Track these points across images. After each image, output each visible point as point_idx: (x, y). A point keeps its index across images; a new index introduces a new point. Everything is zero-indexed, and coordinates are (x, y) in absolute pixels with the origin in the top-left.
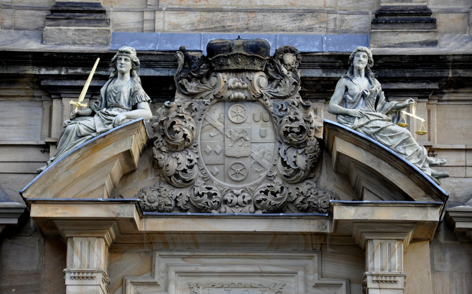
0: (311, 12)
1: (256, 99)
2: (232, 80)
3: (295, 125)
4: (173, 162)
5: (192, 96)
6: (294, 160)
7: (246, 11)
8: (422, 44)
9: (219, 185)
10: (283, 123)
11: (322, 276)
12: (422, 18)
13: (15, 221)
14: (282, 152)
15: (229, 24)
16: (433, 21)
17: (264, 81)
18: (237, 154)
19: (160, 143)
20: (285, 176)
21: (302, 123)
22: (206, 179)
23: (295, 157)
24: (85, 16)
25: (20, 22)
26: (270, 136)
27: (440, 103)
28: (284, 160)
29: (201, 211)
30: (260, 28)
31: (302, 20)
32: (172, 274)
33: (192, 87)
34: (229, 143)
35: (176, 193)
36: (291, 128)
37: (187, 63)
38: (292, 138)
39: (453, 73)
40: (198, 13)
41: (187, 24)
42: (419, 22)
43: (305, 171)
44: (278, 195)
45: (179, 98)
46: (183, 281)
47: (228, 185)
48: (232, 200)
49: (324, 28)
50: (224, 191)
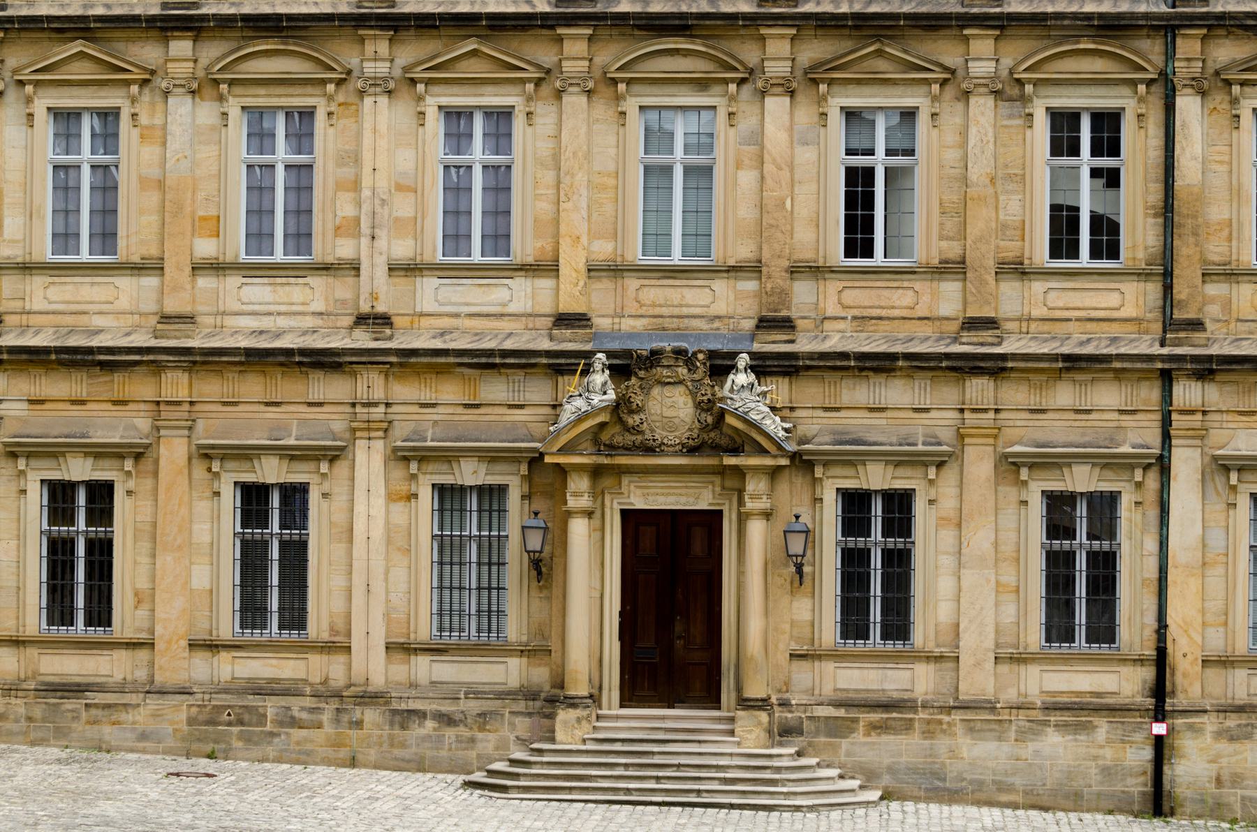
0: (719, 317)
1: (681, 382)
2: (665, 372)
3: (705, 398)
4: (632, 420)
11: (723, 488)
12: (787, 324)
16: (793, 328)
17: (685, 371)
19: (623, 408)
21: (709, 396)
24: (577, 323)
25: (538, 325)
26: (690, 404)
29: (649, 450)
30: (686, 329)
32: (632, 487)
33: (642, 374)
35: (634, 438)
42: (784, 327)
45: (633, 380)
46: (639, 492)
47: (665, 434)
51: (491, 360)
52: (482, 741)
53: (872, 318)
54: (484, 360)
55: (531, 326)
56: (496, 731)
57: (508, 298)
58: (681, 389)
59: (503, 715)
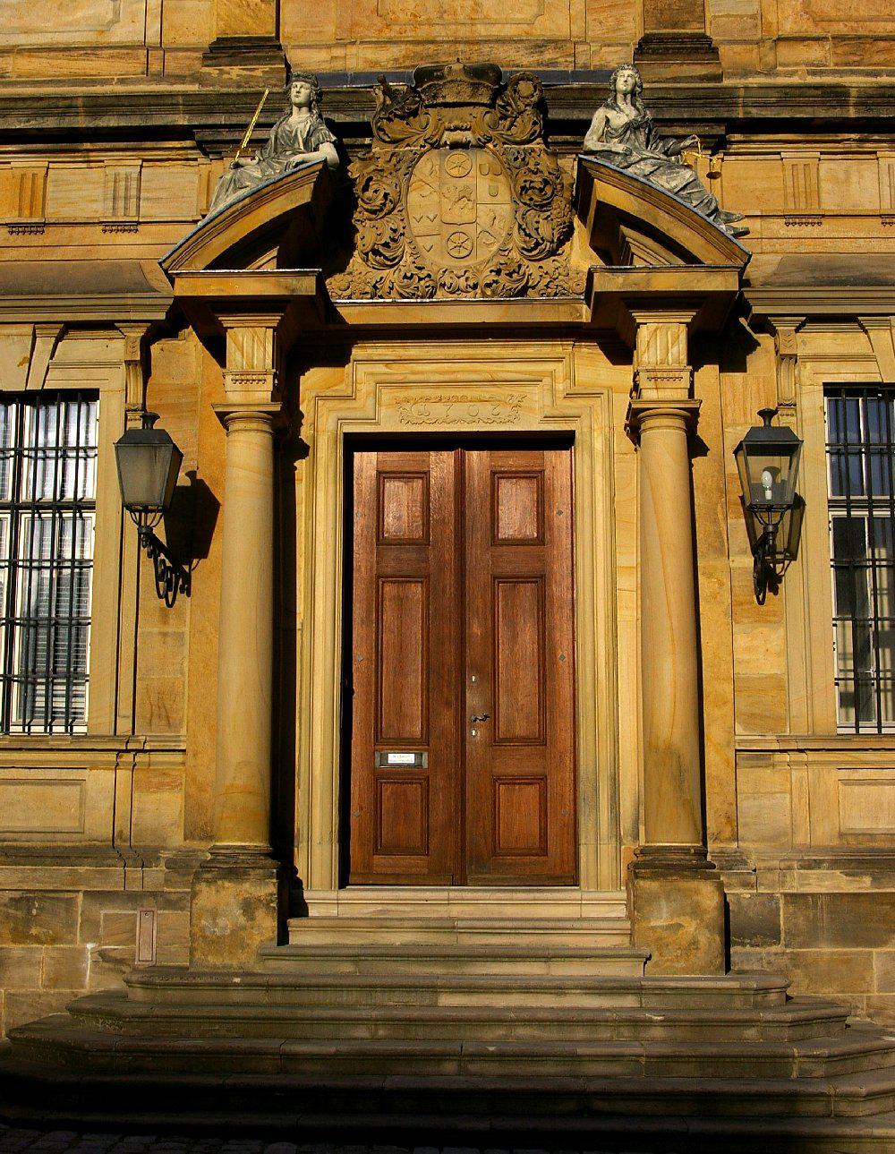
5: (395, 142)
6: (536, 225)
7: (467, 42)
8: (702, 78)
9: (436, 261)
10: (519, 175)
12: (703, 47)
13: (162, 316)
14: (519, 215)
15: (444, 59)
16: (715, 51)
18: (458, 220)
20: (523, 249)
22: (415, 256)
23: (538, 222)
26: (504, 195)
27: (726, 158)
28: (523, 227)
31: (542, 52)
33: (397, 128)
34: (447, 205)
36: (532, 182)
37: (387, 98)
38: (533, 196)
39: (745, 113)
40: (403, 46)
41: (388, 61)
42: (696, 51)
43: (552, 242)
44: (515, 275)
48: (451, 284)
49: (571, 62)
50: (441, 272)
51: (67, 123)
52: (20, 962)
53: (877, 39)
54: (50, 123)
55: (155, 67)
56: (54, 940)
57: (110, 16)
58: (484, 158)
59: (70, 903)
